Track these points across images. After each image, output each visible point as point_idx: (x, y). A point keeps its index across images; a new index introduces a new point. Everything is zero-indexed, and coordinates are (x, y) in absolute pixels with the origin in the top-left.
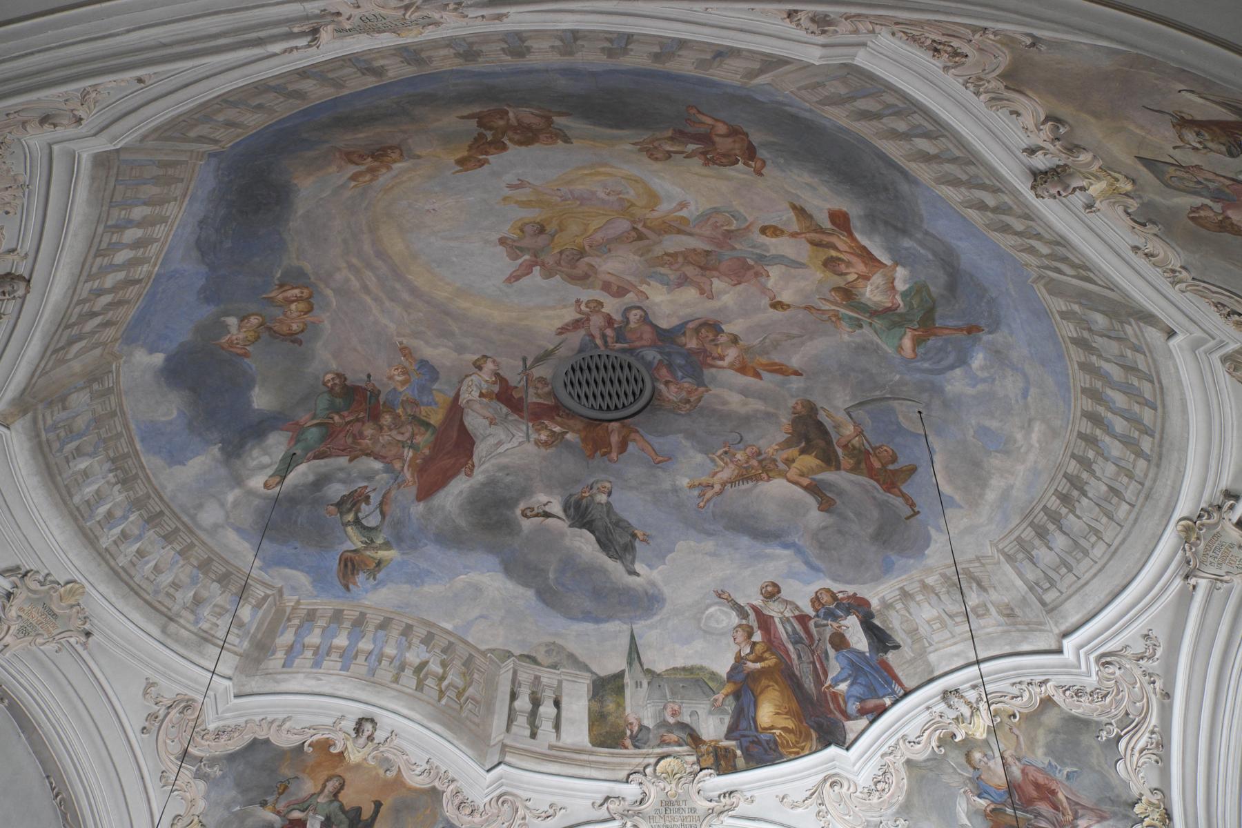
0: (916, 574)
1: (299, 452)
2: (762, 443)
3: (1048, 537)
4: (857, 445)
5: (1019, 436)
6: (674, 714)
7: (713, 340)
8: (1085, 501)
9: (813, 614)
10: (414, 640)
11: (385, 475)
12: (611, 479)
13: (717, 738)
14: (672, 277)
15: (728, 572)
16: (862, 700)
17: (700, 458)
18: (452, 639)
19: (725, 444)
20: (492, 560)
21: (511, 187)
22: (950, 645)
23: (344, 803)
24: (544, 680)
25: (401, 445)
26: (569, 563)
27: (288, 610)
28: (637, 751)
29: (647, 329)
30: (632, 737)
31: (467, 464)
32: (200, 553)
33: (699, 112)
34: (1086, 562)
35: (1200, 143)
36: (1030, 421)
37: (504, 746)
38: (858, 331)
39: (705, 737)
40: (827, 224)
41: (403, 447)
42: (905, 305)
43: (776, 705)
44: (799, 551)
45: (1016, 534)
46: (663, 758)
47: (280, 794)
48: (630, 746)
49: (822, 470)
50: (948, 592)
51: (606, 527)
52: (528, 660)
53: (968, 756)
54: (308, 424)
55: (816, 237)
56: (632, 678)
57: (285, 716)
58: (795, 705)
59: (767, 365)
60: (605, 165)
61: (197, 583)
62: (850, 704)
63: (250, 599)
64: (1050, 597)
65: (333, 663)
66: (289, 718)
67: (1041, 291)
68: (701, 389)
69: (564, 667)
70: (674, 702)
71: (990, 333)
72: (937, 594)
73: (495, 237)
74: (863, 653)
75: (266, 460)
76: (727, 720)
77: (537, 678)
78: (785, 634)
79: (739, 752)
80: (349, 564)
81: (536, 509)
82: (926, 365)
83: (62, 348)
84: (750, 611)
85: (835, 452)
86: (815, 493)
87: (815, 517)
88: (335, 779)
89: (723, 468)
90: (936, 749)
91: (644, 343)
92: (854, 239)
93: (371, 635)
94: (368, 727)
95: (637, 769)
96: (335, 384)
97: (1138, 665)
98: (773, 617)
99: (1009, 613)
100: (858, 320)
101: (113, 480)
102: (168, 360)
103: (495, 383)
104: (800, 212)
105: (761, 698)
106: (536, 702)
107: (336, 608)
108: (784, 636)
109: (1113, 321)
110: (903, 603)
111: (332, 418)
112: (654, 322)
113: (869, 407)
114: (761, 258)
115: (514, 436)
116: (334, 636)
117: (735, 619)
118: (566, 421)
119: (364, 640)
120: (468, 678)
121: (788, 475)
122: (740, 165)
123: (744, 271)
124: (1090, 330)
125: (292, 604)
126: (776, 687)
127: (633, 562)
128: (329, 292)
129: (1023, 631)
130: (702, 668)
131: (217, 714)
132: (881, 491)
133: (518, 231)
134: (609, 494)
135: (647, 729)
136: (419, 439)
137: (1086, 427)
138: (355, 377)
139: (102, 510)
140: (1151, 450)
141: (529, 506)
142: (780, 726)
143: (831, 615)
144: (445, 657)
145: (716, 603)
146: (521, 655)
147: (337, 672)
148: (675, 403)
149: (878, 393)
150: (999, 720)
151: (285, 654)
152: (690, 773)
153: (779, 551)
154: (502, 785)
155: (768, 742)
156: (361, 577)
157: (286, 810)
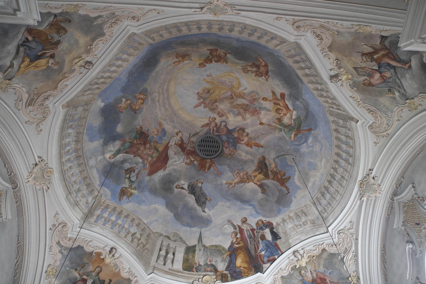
0: (287, 213)
1: (122, 149)
2: (248, 170)
3: (325, 196)
4: (275, 171)
5: (319, 164)
6: (210, 261)
7: (242, 134)
8: (335, 182)
9: (256, 228)
10: (134, 224)
11: (142, 164)
12: (204, 179)
13: (223, 270)
14: (236, 112)
15: (232, 213)
16: (268, 257)
17: (230, 174)
18: (145, 227)
19: (238, 170)
20: (163, 201)
21: (208, 76)
22: (296, 236)
23: (100, 277)
24: (171, 245)
25: (149, 155)
26: (186, 206)
27: (102, 202)
28: (197, 273)
29: (225, 129)
30: (196, 268)
31: (165, 166)
32: (85, 173)
33: (260, 57)
34: (335, 202)
35: (366, 60)
36: (322, 158)
37: (154, 267)
38: (281, 133)
39: (219, 270)
40: (279, 97)
41: (149, 156)
42: (294, 123)
43: (242, 259)
44: (254, 207)
45: (316, 196)
46: (205, 276)
47: (82, 268)
48: (195, 271)
49: (264, 179)
50: (296, 218)
51: (199, 195)
52: (167, 238)
53: (300, 272)
54: (128, 141)
55: (275, 101)
56: (198, 248)
57: (90, 240)
58: (248, 259)
59: (255, 144)
60: (232, 72)
61: (80, 184)
62: (265, 259)
63: (93, 195)
64: (324, 215)
65: (109, 225)
66: (91, 241)
67: (328, 114)
68: (235, 151)
69: (178, 242)
70: (211, 257)
71: (314, 130)
72: (293, 219)
73: (196, 92)
74: (270, 241)
75: (113, 149)
76: (226, 264)
77: (169, 244)
78: (247, 235)
79: (229, 275)
80: (123, 192)
81: (180, 186)
82: (297, 143)
83: (85, 91)
84: (237, 227)
85: (268, 173)
86: (261, 187)
87: (260, 195)
88: (99, 268)
89: (236, 178)
90: (290, 271)
91: (223, 133)
92: (285, 102)
93: (122, 219)
94: (114, 250)
95: (196, 279)
96: (139, 130)
97: (348, 232)
98: (244, 229)
99: (313, 222)
100: (281, 129)
101: (74, 140)
102: (104, 106)
103: (180, 141)
104: (274, 93)
105: (238, 257)
106: (167, 253)
107: (115, 206)
108: (247, 236)
109: (344, 122)
110: (283, 223)
111: (134, 141)
112: (228, 127)
113: (280, 158)
114: (260, 108)
115: (180, 159)
116: (112, 216)
117: (232, 230)
118: (196, 157)
119: (120, 220)
120: (147, 241)
121: (254, 181)
122: (263, 77)
123: (256, 112)
124: (338, 126)
125: (103, 201)
126: (243, 253)
127: (204, 208)
128: (150, 99)
129: (317, 228)
130: (220, 246)
131: (72, 232)
132: (280, 186)
133: (203, 91)
134: (202, 184)
135: (201, 265)
136: (154, 155)
137: (336, 158)
138: (145, 129)
139: (68, 148)
140: (352, 162)
141: (178, 184)
142: (243, 266)
143: (262, 229)
144: (142, 232)
145: (227, 224)
146: (165, 236)
147: (109, 229)
148: (227, 155)
149: (283, 153)
150: (309, 259)
151: (96, 218)
152: (213, 282)
153: (248, 207)
154: (151, 281)
155: (239, 272)
156: (125, 197)
157: (82, 274)
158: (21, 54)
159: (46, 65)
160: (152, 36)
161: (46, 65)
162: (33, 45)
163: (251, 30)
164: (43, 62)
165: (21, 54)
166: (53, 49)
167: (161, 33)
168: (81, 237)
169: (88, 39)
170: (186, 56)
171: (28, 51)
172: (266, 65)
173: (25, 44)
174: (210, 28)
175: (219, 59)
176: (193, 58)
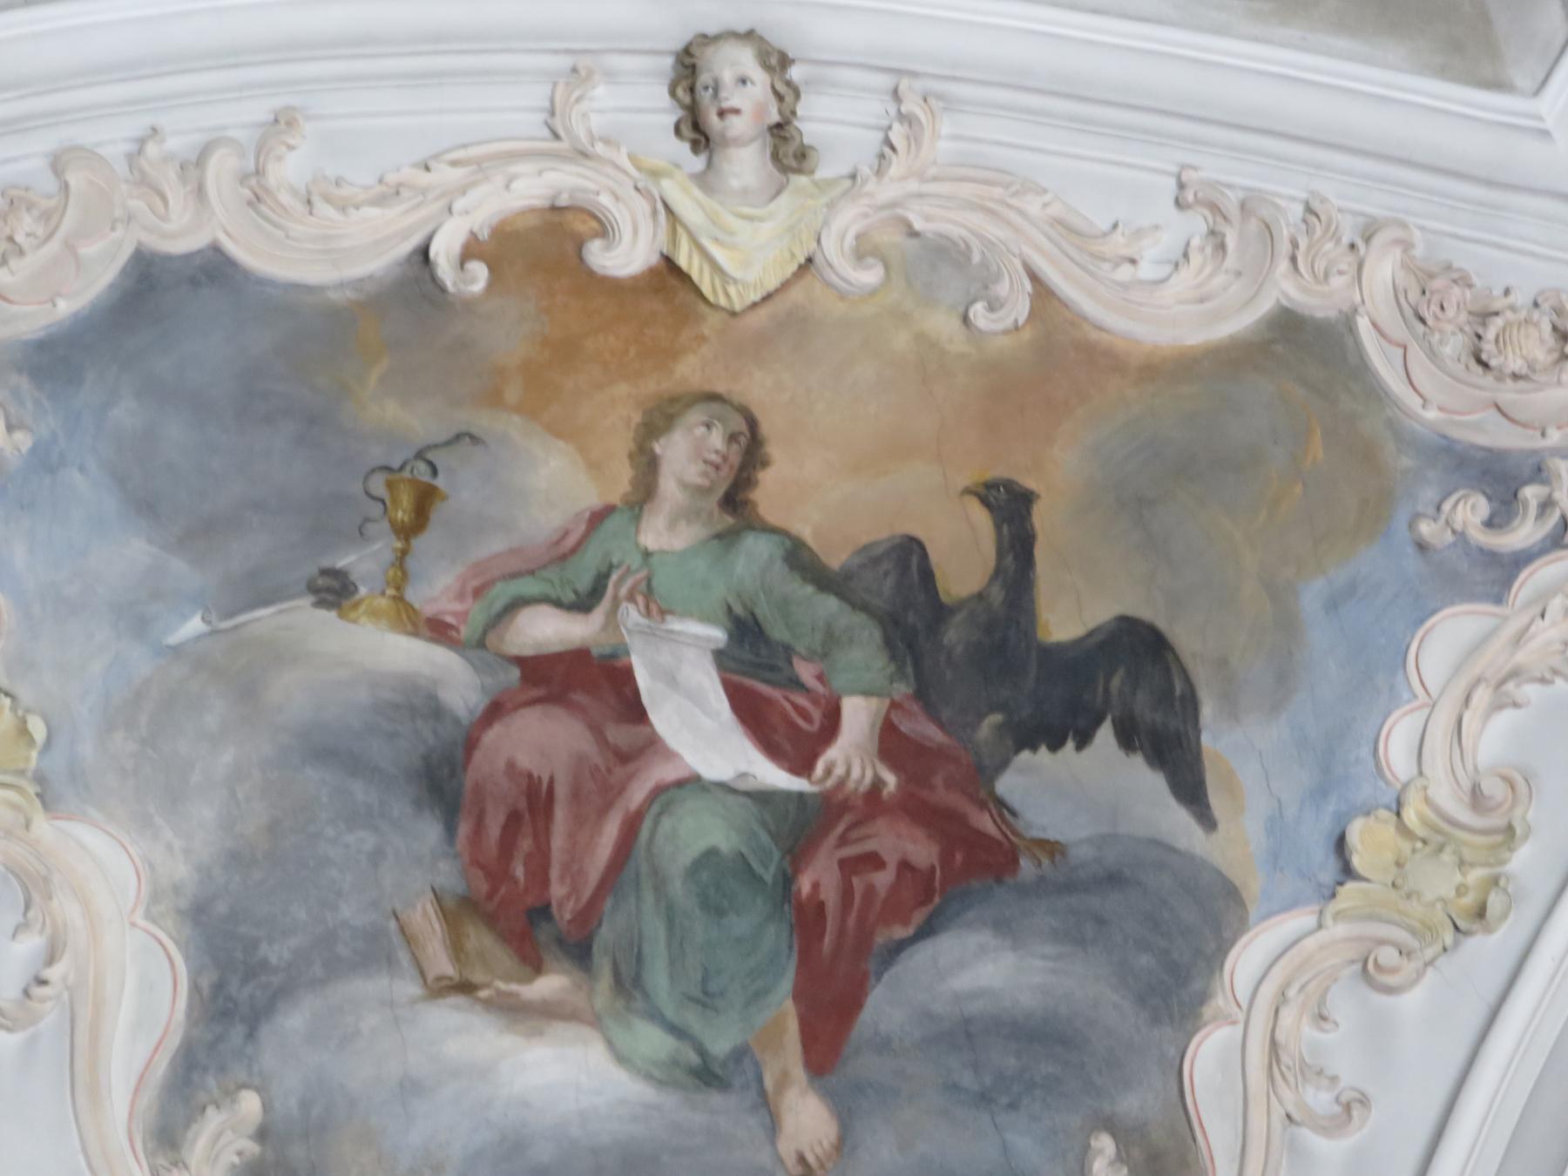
23: (805, 532)
57: (259, 110)
66: (283, 122)
88: (696, 416)
157: (478, 614)
168: (84, 135)
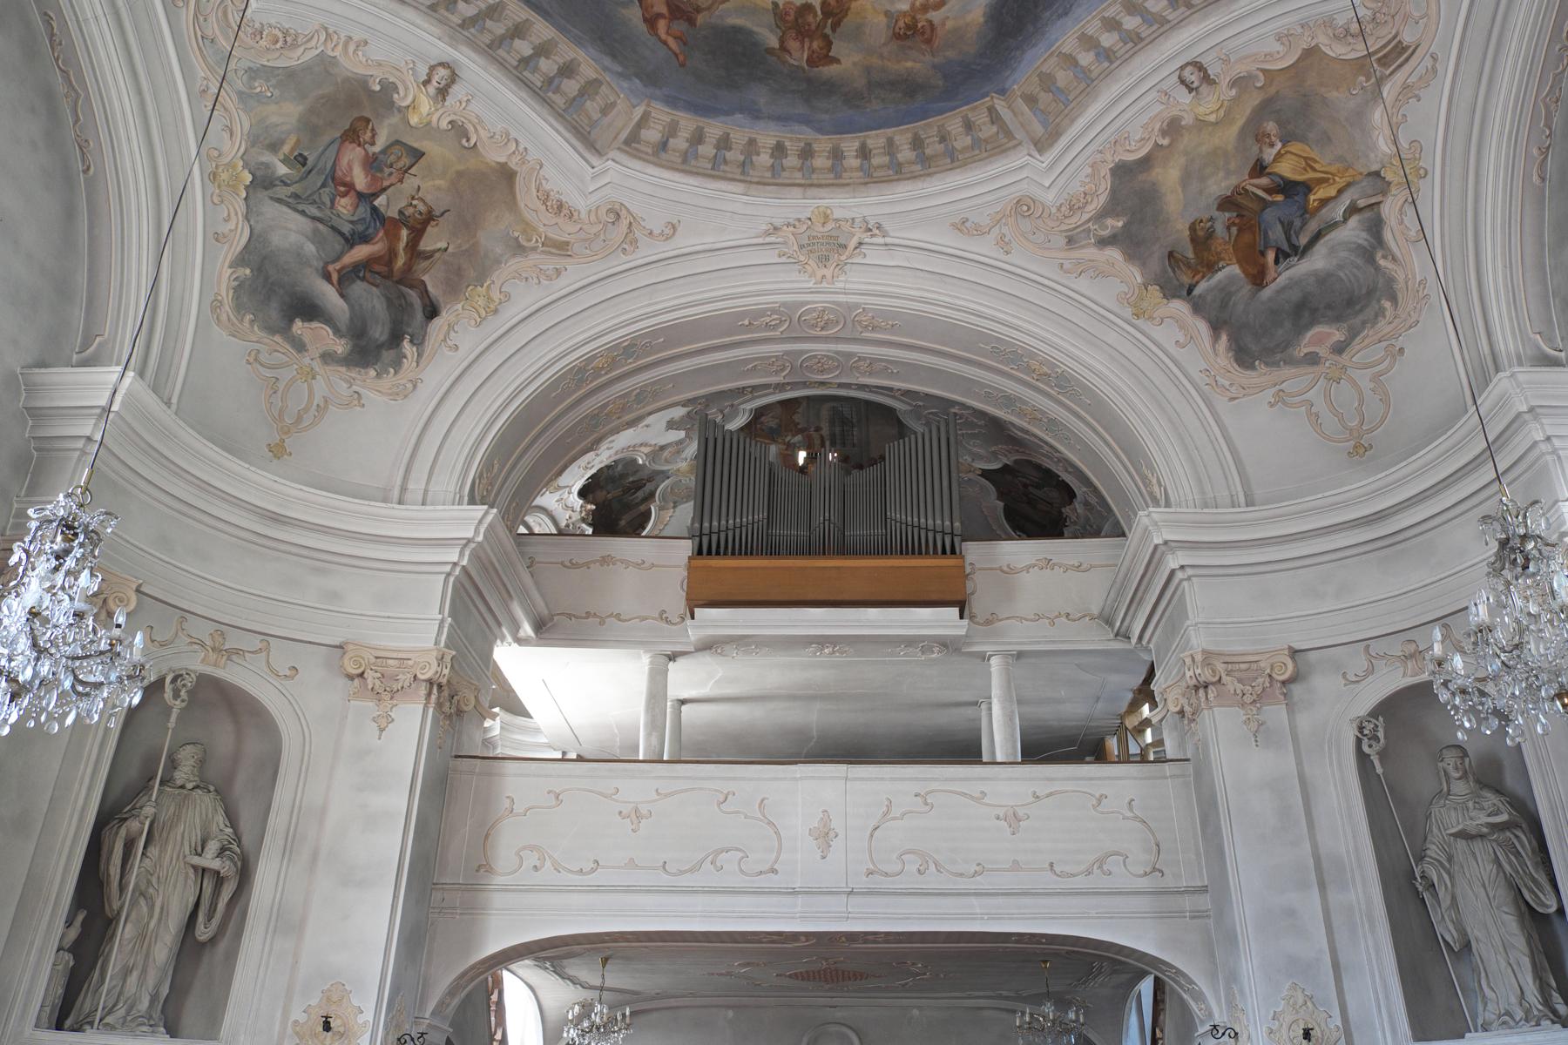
33: (676, 55)
158: (1313, 226)
159: (1287, 152)
160: (994, 129)
161: (1287, 152)
162: (1277, 234)
163: (725, 162)
164: (1287, 169)
165: (1313, 226)
166: (1246, 191)
167: (968, 140)
169: (1157, 173)
170: (905, 34)
171: (1297, 223)
172: (651, 21)
173: (1288, 250)
174: (837, 155)
175: (800, 21)
176: (882, 20)
